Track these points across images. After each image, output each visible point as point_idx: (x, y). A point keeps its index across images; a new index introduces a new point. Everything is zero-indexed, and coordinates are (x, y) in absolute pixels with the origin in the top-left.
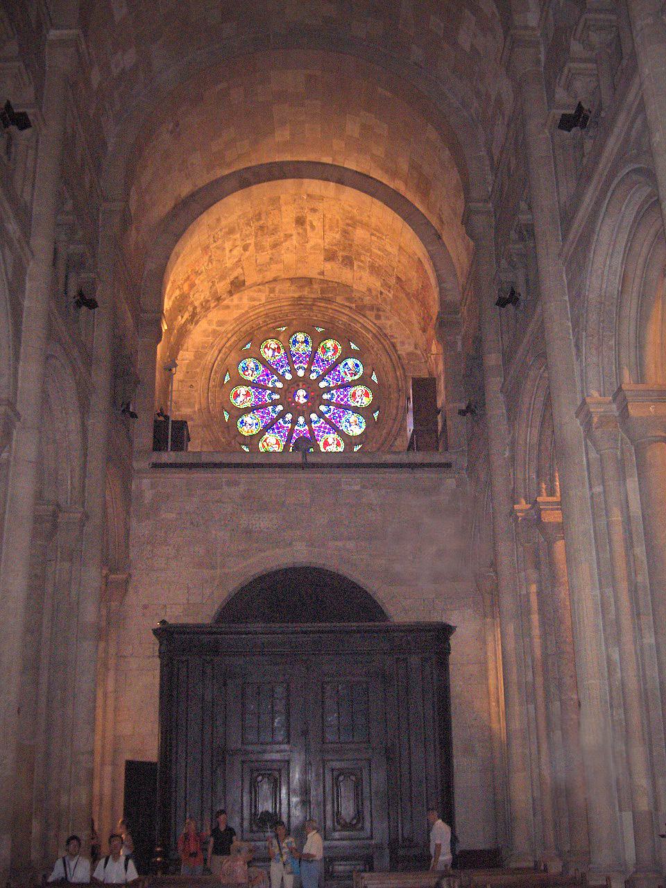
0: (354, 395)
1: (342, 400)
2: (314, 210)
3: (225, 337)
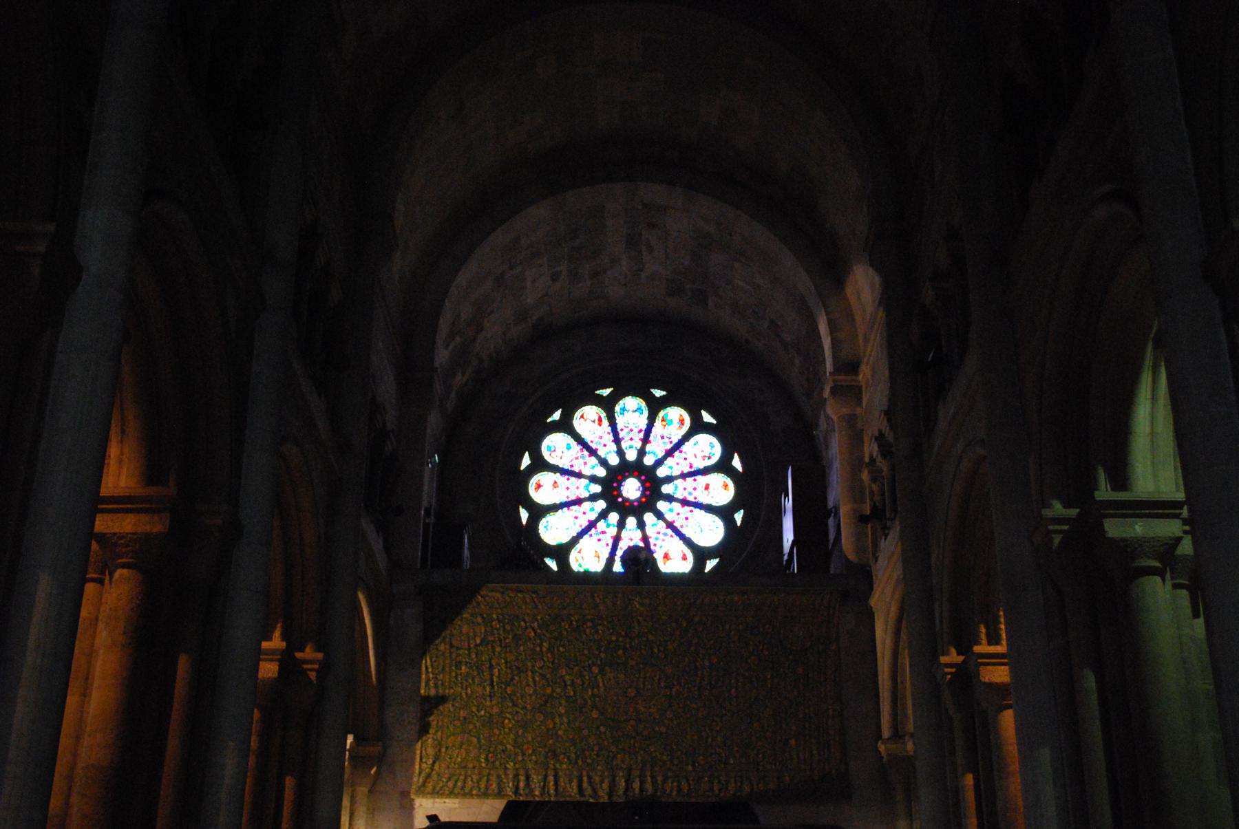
0: (707, 487)
2: (652, 225)
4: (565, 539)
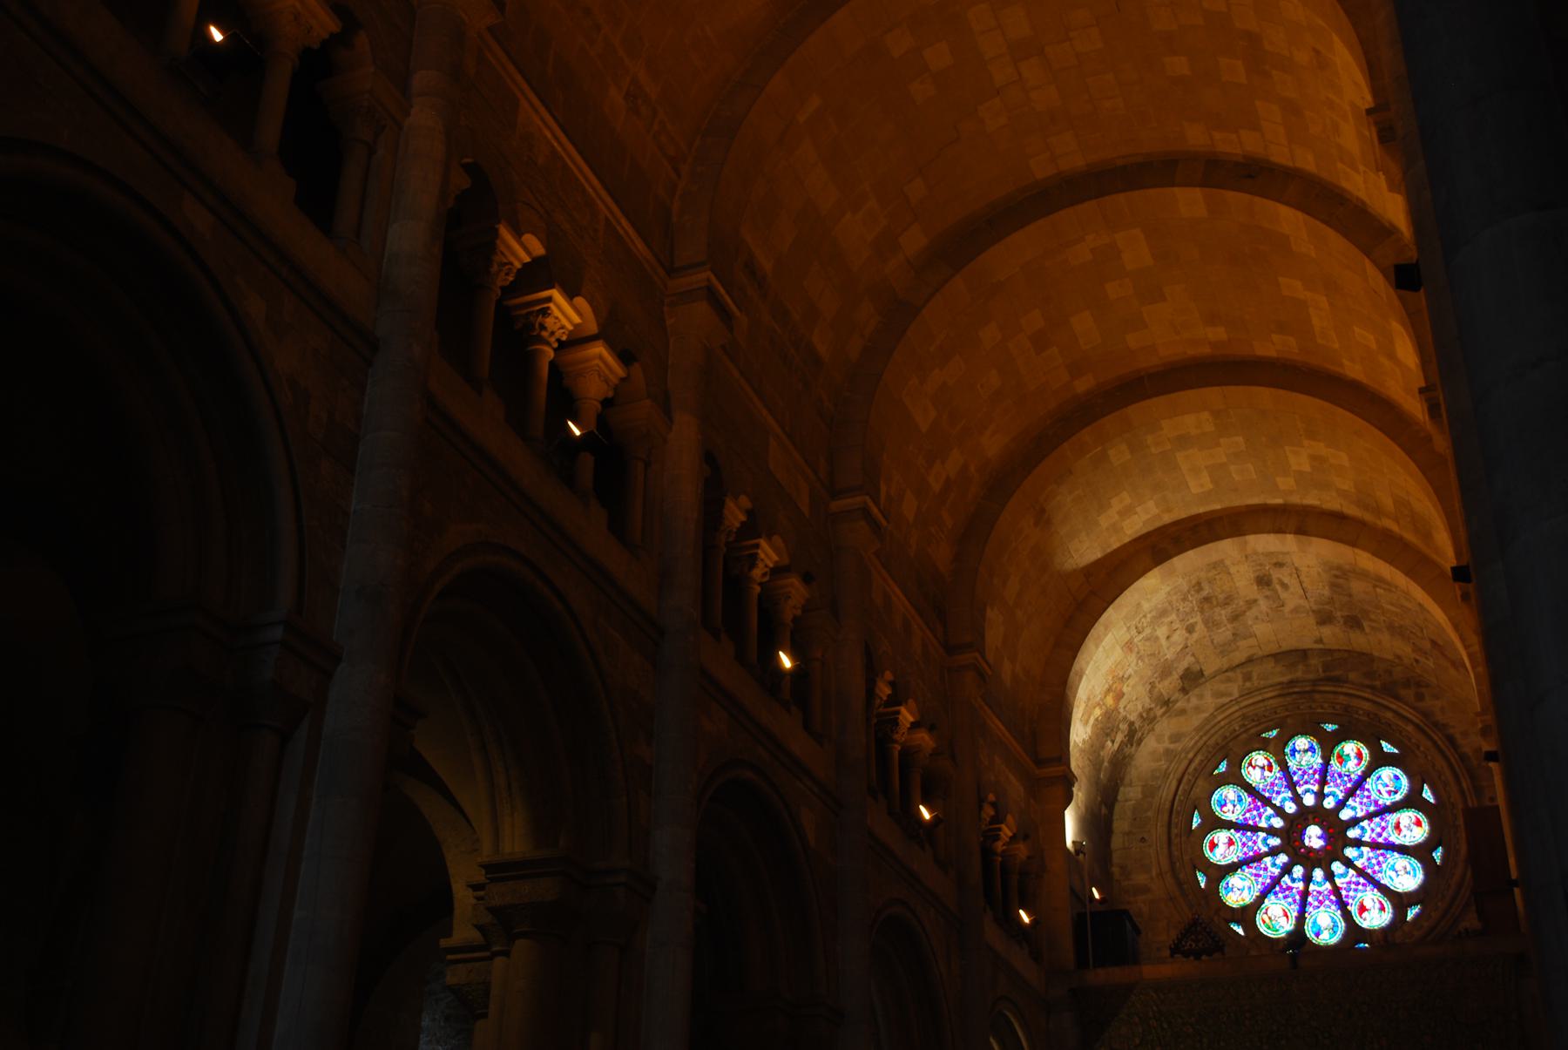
0: (1397, 827)
1: (1380, 835)
2: (1279, 565)
3: (1186, 757)
4: (1247, 898)
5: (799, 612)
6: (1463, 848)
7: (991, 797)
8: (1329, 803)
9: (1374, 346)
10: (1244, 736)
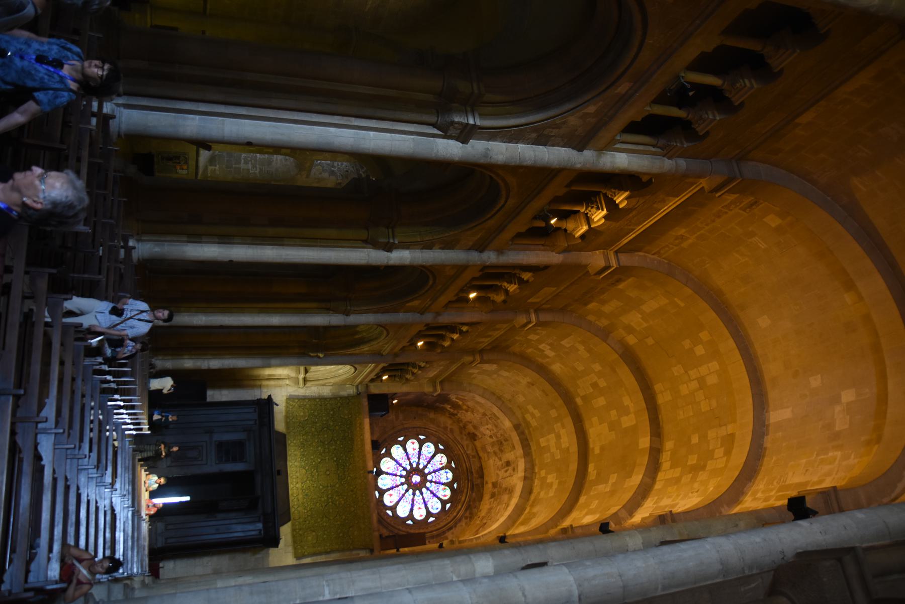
0: (419, 508)
1: (417, 502)
2: (514, 470)
4: (394, 455)
5: (491, 299)
6: (412, 531)
7: (428, 366)
8: (428, 484)
9: (591, 507)
10: (452, 455)
